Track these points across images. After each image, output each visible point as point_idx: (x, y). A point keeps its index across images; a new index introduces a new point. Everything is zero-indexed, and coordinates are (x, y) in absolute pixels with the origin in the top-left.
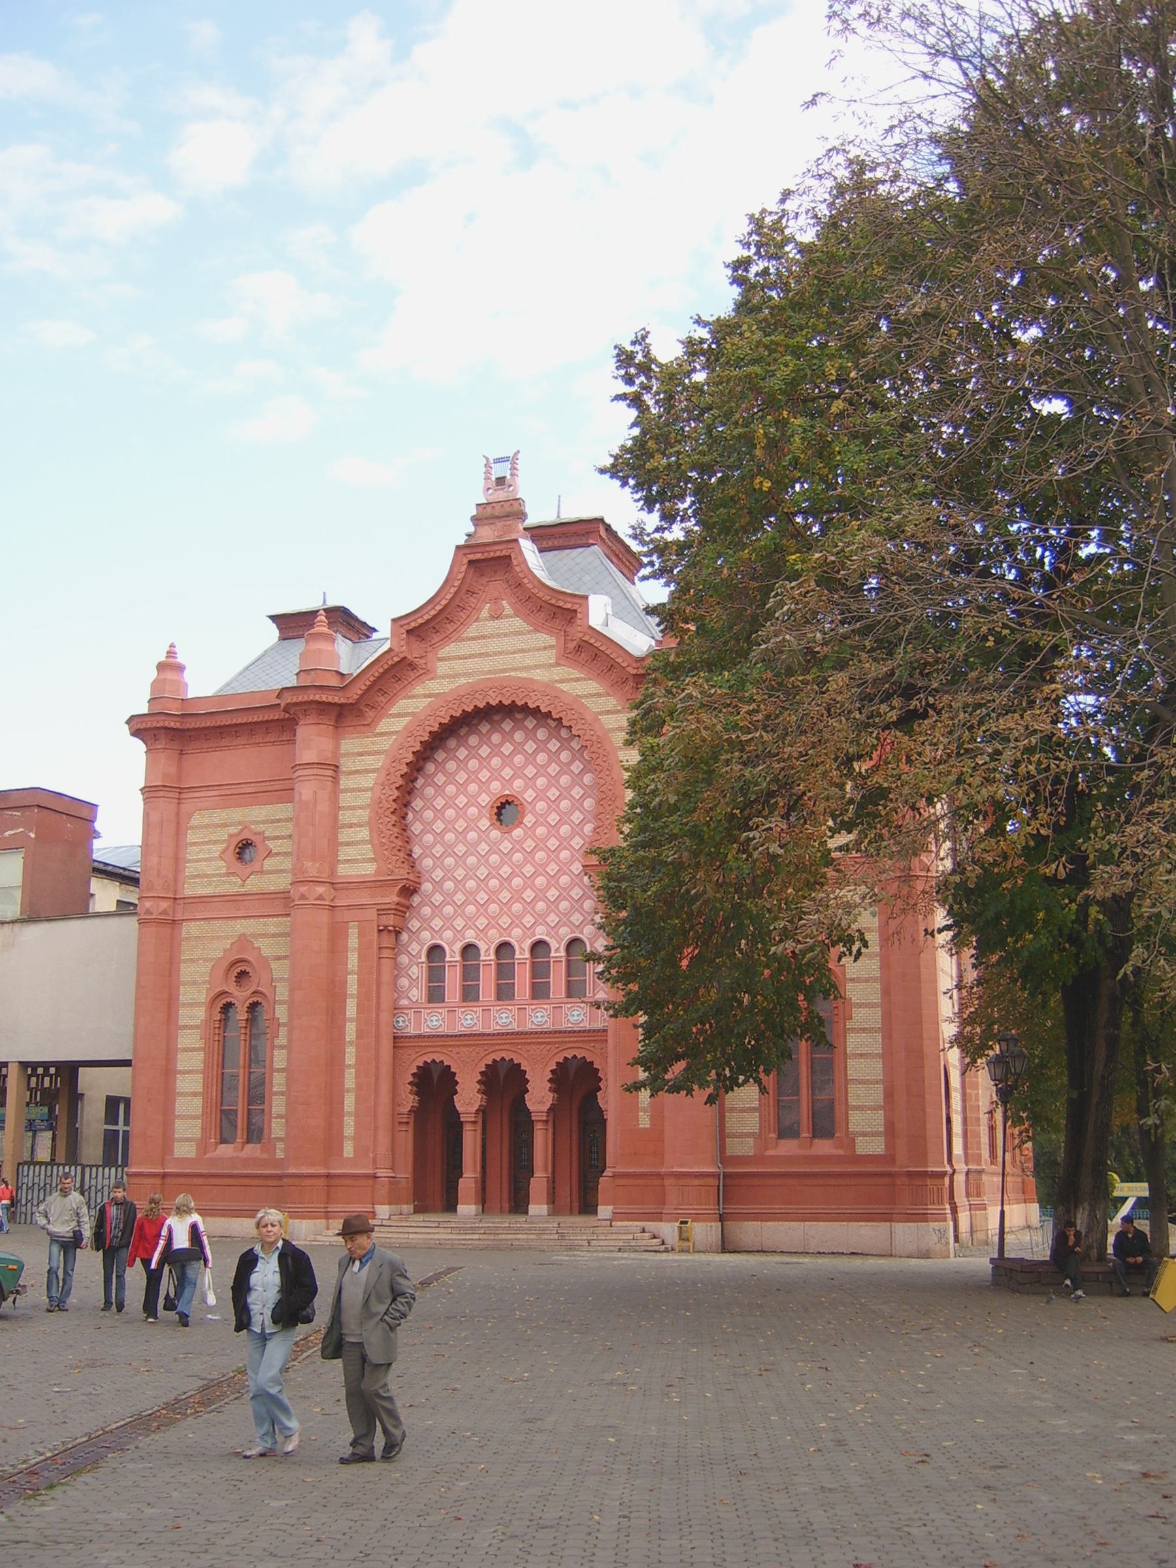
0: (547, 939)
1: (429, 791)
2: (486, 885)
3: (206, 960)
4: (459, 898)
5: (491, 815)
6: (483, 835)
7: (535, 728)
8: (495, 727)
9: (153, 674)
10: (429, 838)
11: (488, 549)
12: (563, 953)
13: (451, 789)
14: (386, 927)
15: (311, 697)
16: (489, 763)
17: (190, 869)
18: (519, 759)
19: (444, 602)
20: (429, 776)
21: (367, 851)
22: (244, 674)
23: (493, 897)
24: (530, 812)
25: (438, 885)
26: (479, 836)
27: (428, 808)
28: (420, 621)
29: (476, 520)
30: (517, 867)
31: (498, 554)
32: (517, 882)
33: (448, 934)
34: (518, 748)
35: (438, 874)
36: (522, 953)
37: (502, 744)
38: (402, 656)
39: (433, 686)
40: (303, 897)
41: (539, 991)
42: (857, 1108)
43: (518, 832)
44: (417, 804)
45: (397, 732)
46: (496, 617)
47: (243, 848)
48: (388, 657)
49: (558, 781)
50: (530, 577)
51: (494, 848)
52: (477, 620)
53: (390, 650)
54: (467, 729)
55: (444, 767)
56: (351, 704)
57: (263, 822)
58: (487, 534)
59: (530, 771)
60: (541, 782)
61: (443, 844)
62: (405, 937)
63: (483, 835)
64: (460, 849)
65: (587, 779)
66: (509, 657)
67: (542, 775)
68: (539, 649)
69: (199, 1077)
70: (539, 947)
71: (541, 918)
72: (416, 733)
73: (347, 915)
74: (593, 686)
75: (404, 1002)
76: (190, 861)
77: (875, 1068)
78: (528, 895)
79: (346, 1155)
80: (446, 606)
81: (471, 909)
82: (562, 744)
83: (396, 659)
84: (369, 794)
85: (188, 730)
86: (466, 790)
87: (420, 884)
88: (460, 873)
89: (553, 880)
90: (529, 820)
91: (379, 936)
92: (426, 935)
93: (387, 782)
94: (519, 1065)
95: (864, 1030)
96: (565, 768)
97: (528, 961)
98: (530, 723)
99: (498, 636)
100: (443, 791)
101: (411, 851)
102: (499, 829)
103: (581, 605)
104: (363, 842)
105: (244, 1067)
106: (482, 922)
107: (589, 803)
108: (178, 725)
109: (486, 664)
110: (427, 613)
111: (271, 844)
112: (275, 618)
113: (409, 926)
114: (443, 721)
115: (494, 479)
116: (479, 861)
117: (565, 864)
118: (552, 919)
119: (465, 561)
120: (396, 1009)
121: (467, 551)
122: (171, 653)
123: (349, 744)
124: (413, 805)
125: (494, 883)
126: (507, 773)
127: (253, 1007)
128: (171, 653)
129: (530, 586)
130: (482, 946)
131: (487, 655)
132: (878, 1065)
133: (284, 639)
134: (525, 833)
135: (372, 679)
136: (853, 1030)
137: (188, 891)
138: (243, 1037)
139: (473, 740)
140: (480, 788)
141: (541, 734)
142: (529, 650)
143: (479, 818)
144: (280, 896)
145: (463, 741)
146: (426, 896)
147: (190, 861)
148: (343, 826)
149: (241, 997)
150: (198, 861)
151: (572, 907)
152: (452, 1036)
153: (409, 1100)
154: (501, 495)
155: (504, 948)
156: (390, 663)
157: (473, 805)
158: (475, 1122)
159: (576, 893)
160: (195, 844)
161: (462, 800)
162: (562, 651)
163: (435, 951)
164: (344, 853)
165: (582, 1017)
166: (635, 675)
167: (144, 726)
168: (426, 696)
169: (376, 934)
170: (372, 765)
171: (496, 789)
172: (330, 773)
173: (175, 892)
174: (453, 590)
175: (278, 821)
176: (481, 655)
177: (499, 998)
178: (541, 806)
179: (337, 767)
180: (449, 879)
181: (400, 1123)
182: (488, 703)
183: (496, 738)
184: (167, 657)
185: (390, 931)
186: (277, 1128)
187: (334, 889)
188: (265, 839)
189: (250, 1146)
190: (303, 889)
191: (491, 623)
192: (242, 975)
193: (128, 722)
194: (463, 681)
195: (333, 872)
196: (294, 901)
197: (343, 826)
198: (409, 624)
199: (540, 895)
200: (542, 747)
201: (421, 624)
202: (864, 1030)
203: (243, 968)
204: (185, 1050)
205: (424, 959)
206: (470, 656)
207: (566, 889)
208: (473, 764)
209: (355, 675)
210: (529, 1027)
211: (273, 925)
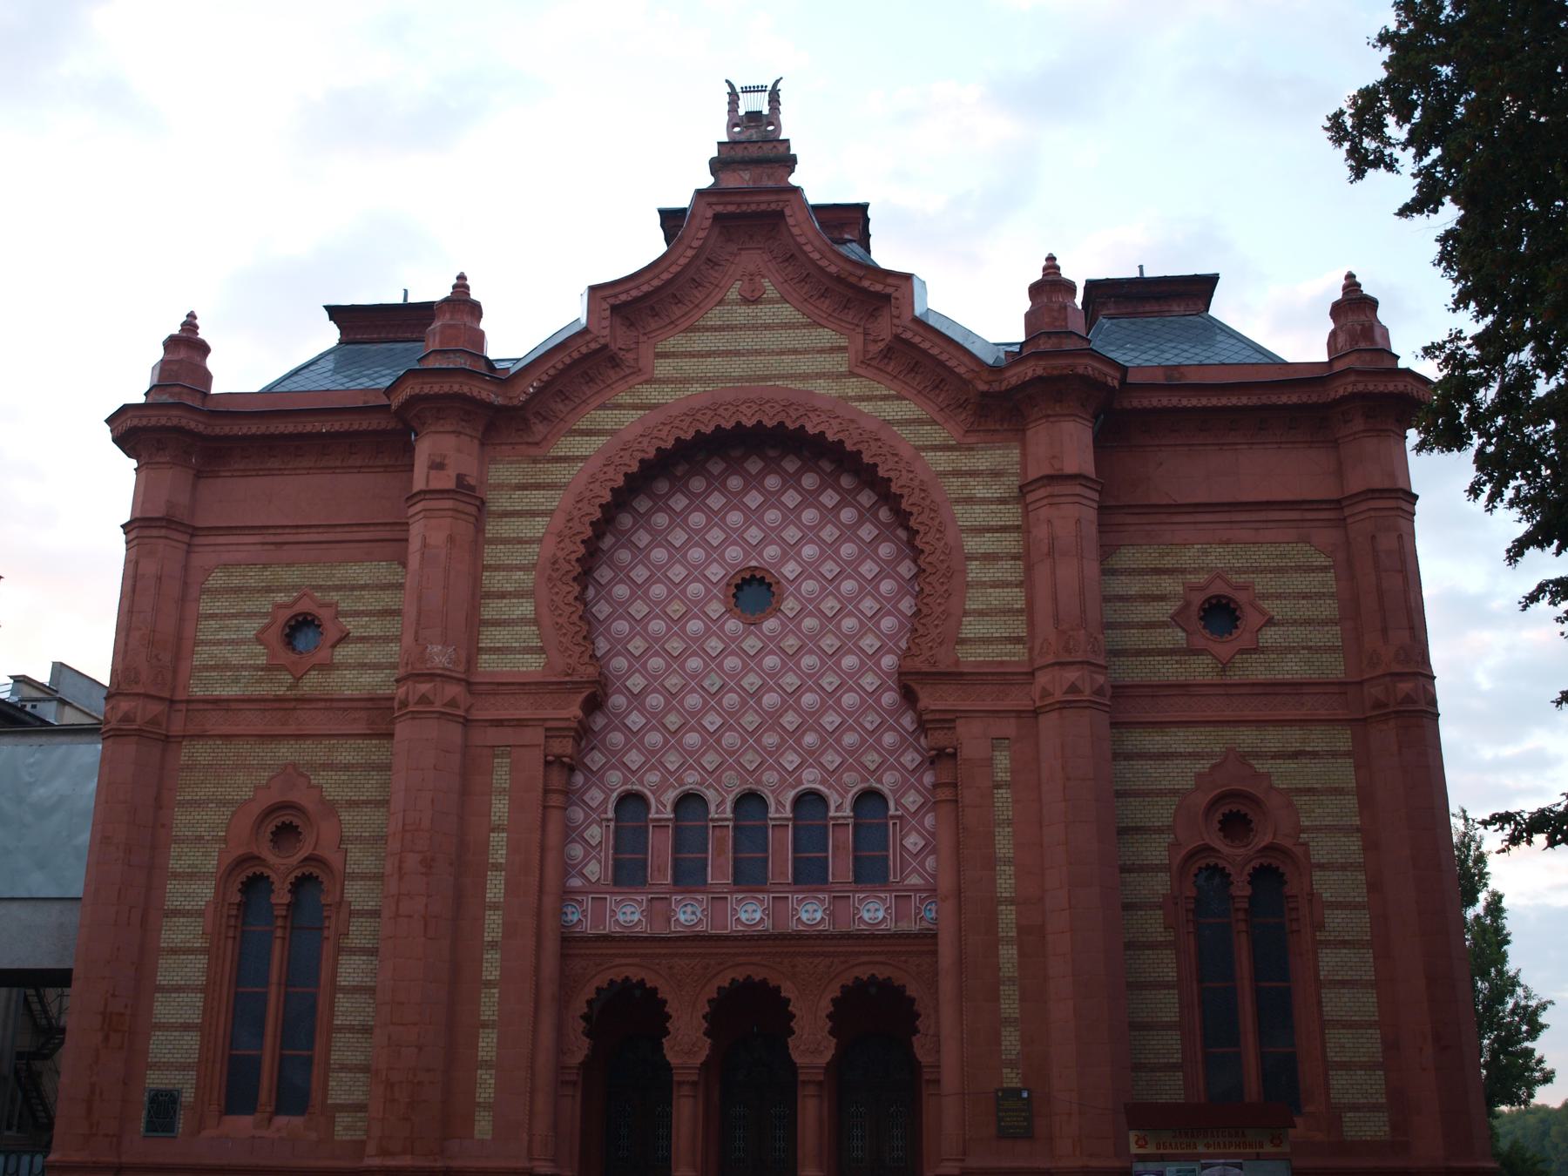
0: (821, 788)
1: (624, 556)
2: (719, 703)
3: (223, 803)
4: (673, 721)
5: (726, 596)
6: (713, 627)
7: (799, 473)
8: (735, 467)
9: (159, 353)
10: (622, 626)
11: (747, 199)
12: (848, 812)
13: (659, 555)
14: (558, 757)
15: (456, 388)
16: (723, 519)
17: (202, 656)
18: (772, 516)
19: (674, 269)
20: (624, 533)
21: (528, 634)
22: (294, 379)
23: (731, 720)
24: (791, 593)
25: (637, 699)
26: (708, 628)
27: (621, 581)
28: (634, 293)
29: (716, 166)
30: (771, 676)
31: (763, 207)
32: (770, 700)
33: (653, 778)
34: (771, 499)
35: (636, 682)
36: (780, 808)
37: (745, 491)
38: (602, 341)
39: (653, 394)
40: (424, 700)
41: (810, 874)
42: (1344, 1066)
43: (770, 624)
44: (604, 574)
45: (584, 458)
46: (751, 300)
47: (300, 625)
48: (580, 341)
49: (837, 552)
50: (817, 243)
51: (732, 646)
52: (721, 302)
53: (584, 332)
54: (687, 467)
55: (648, 521)
56: (515, 408)
57: (337, 588)
58: (741, 179)
59: (792, 534)
60: (809, 551)
61: (645, 635)
62: (579, 779)
63: (713, 627)
64: (675, 646)
65: (885, 550)
66: (773, 359)
67: (811, 541)
68: (821, 351)
69: (197, 999)
70: (810, 801)
71: (811, 757)
72: (617, 460)
73: (493, 736)
74: (906, 409)
75: (576, 882)
76: (203, 643)
77: (1366, 1004)
78: (790, 720)
79: (477, 1136)
80: (677, 275)
81: (692, 739)
82: (843, 499)
83: (594, 346)
84: (536, 548)
85: (217, 438)
86: (684, 556)
87: (606, 694)
88: (673, 682)
89: (831, 699)
90: (790, 606)
91: (545, 771)
92: (614, 777)
93: (567, 532)
94: (777, 989)
95: (1344, 944)
96: (848, 533)
97: (790, 824)
98: (791, 465)
99: (754, 328)
100: (647, 556)
101: (593, 643)
102: (739, 618)
103: (897, 288)
104: (523, 621)
105: (279, 984)
106: (711, 760)
107: (886, 586)
108: (201, 428)
109: (737, 367)
110: (648, 282)
111: (350, 624)
112: (337, 313)
113: (587, 760)
114: (703, 429)
115: (741, 112)
116: (706, 665)
117: (851, 676)
118: (831, 759)
119: (709, 213)
120: (567, 895)
121: (714, 200)
122: (190, 324)
123: (504, 472)
124: (596, 575)
125: (731, 699)
126: (754, 535)
127: (303, 884)
128: (190, 324)
129: (816, 256)
130: (711, 796)
131: (737, 353)
132: (1370, 999)
133: (347, 343)
134: (783, 625)
135: (552, 372)
136: (1327, 944)
137: (198, 692)
138: (279, 933)
139: (697, 484)
140: (708, 555)
141: (809, 481)
142: (805, 351)
143: (709, 597)
144: (362, 704)
145: (679, 485)
146: (617, 715)
147: (203, 643)
148: (489, 595)
149: (281, 865)
150: (219, 643)
151: (864, 741)
152: (663, 939)
153: (581, 1049)
154: (753, 134)
155: (750, 801)
156: (584, 350)
157: (696, 580)
158: (694, 1084)
159: (871, 720)
160: (212, 616)
161: (677, 573)
162: (861, 358)
163: (632, 802)
164: (489, 638)
165: (880, 915)
166: (984, 394)
167: (144, 422)
168: (635, 407)
169: (541, 768)
170: (543, 503)
171: (734, 558)
172: (473, 510)
173: (173, 689)
174: (690, 253)
175: (363, 587)
176: (727, 353)
177: (736, 882)
178: (809, 586)
179: (483, 502)
180: (655, 690)
181: (562, 1082)
182: (739, 423)
183: (735, 483)
184: (182, 330)
185: (563, 764)
186: (342, 1089)
187: (470, 692)
188: (338, 614)
189: (281, 1120)
190: (424, 687)
191: (743, 309)
192: (286, 833)
193: (109, 421)
194: (697, 388)
195: (471, 662)
196: (406, 706)
197: (489, 595)
198: (616, 296)
199: (810, 721)
200: (810, 499)
201: (636, 300)
202: (1344, 944)
203: (287, 819)
204: (174, 951)
205: (611, 815)
206: (709, 354)
207: (852, 713)
208: (697, 519)
209: (512, 371)
210: (793, 926)
211: (346, 753)
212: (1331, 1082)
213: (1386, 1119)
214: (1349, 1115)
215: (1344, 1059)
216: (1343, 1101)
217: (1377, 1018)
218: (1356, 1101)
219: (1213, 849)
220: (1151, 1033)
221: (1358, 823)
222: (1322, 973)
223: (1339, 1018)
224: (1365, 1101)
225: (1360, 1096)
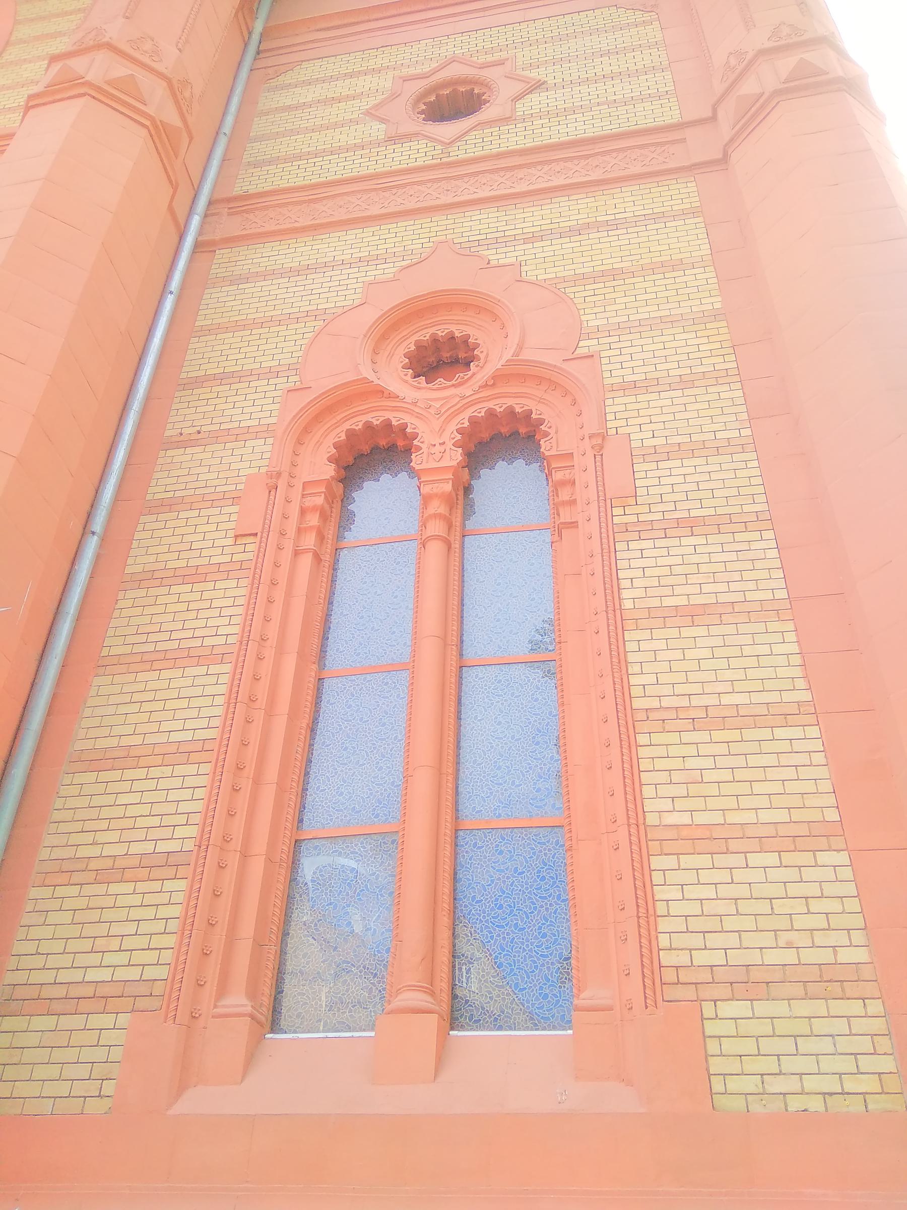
95: (691, 525)
202: (691, 525)
212: (661, 893)
213: (878, 1025)
214: (728, 1009)
215: (700, 818)
216: (701, 958)
217: (806, 696)
218: (754, 957)
219: (380, 392)
220: (129, 774)
221: (718, 306)
222: (625, 594)
223: (684, 702)
224: (790, 957)
225: (767, 939)
